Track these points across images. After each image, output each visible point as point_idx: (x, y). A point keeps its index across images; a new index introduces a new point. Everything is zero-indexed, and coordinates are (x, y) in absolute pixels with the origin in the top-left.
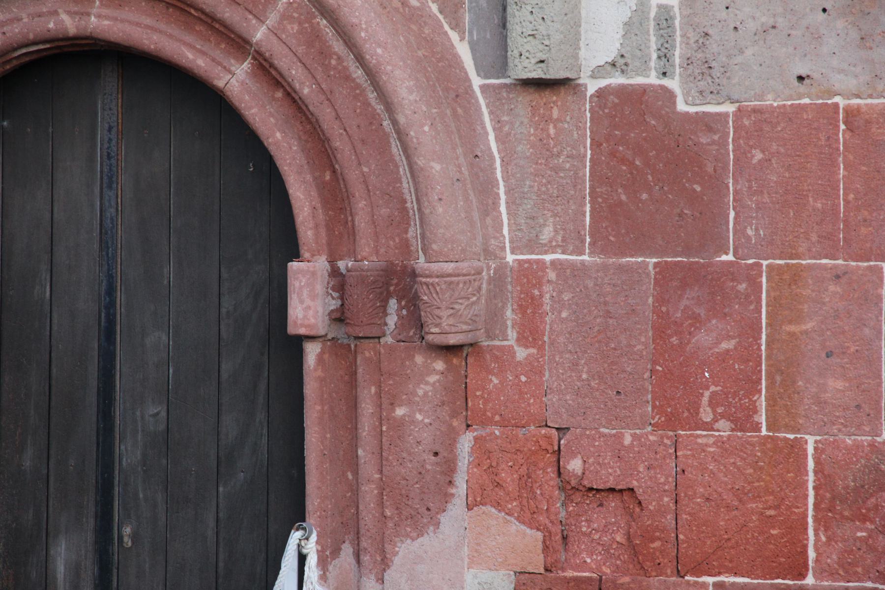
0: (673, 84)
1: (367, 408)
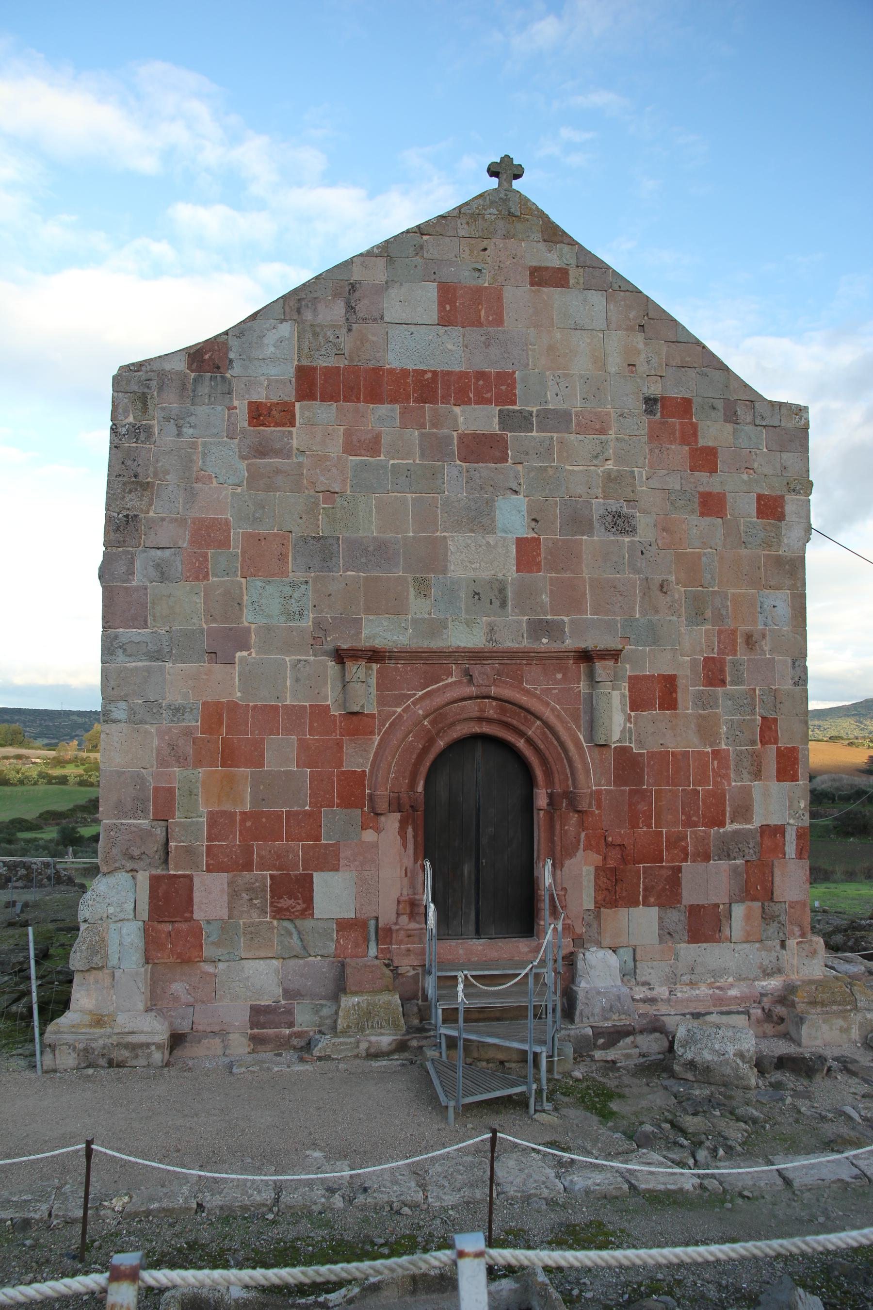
0: (633, 745)
1: (558, 827)
